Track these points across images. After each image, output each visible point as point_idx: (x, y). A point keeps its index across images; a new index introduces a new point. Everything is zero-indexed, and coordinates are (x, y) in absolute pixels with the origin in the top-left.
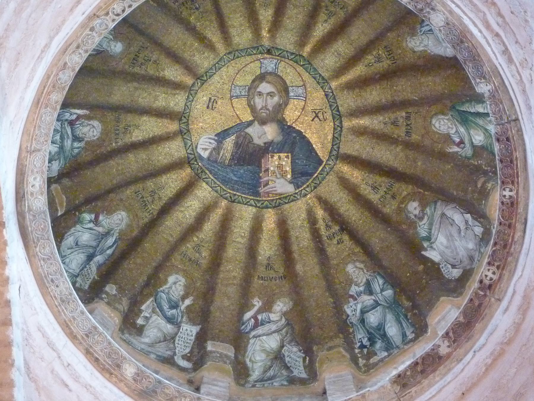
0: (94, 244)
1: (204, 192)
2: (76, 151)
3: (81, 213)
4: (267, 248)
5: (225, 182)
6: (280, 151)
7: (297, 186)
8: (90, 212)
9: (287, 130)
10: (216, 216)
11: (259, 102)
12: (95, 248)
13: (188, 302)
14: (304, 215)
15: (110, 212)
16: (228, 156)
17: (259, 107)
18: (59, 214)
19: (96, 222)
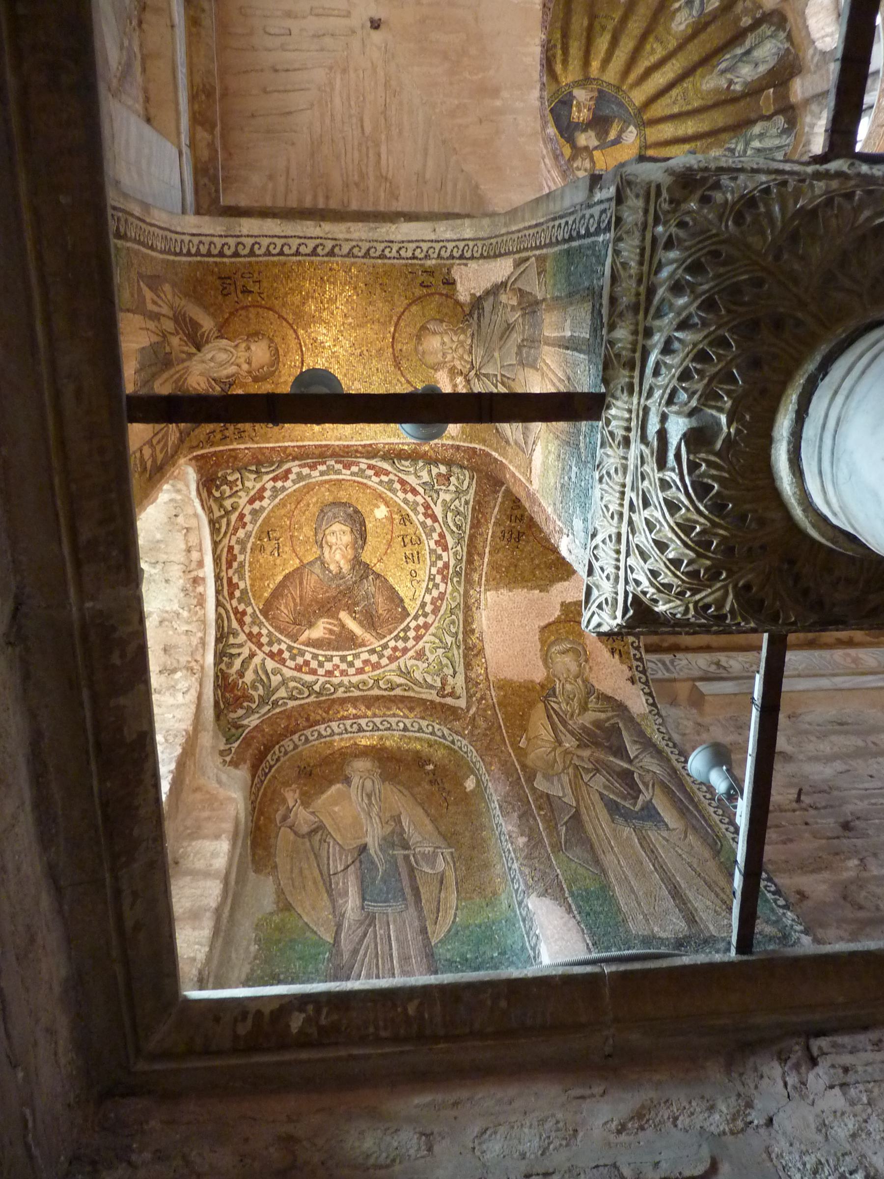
0: (740, 64)
1: (638, 96)
2: (734, 141)
3: (743, 91)
4: (602, 43)
5: (621, 105)
6: (578, 123)
7: (571, 93)
8: (734, 91)
9: (571, 140)
10: (633, 77)
11: (587, 164)
12: (740, 60)
13: (677, 5)
14: (571, 68)
15: (717, 91)
16: (615, 125)
17: (587, 161)
18: (772, 90)
19: (731, 82)
